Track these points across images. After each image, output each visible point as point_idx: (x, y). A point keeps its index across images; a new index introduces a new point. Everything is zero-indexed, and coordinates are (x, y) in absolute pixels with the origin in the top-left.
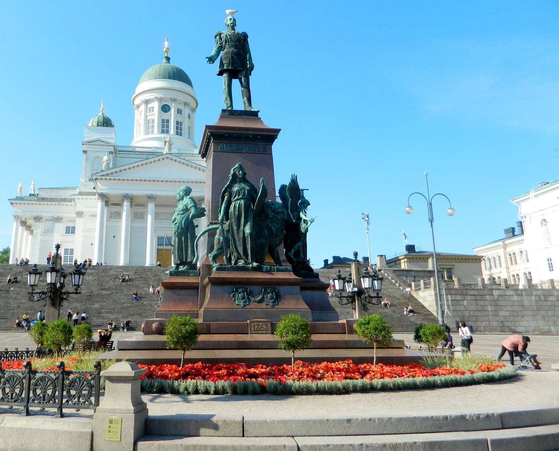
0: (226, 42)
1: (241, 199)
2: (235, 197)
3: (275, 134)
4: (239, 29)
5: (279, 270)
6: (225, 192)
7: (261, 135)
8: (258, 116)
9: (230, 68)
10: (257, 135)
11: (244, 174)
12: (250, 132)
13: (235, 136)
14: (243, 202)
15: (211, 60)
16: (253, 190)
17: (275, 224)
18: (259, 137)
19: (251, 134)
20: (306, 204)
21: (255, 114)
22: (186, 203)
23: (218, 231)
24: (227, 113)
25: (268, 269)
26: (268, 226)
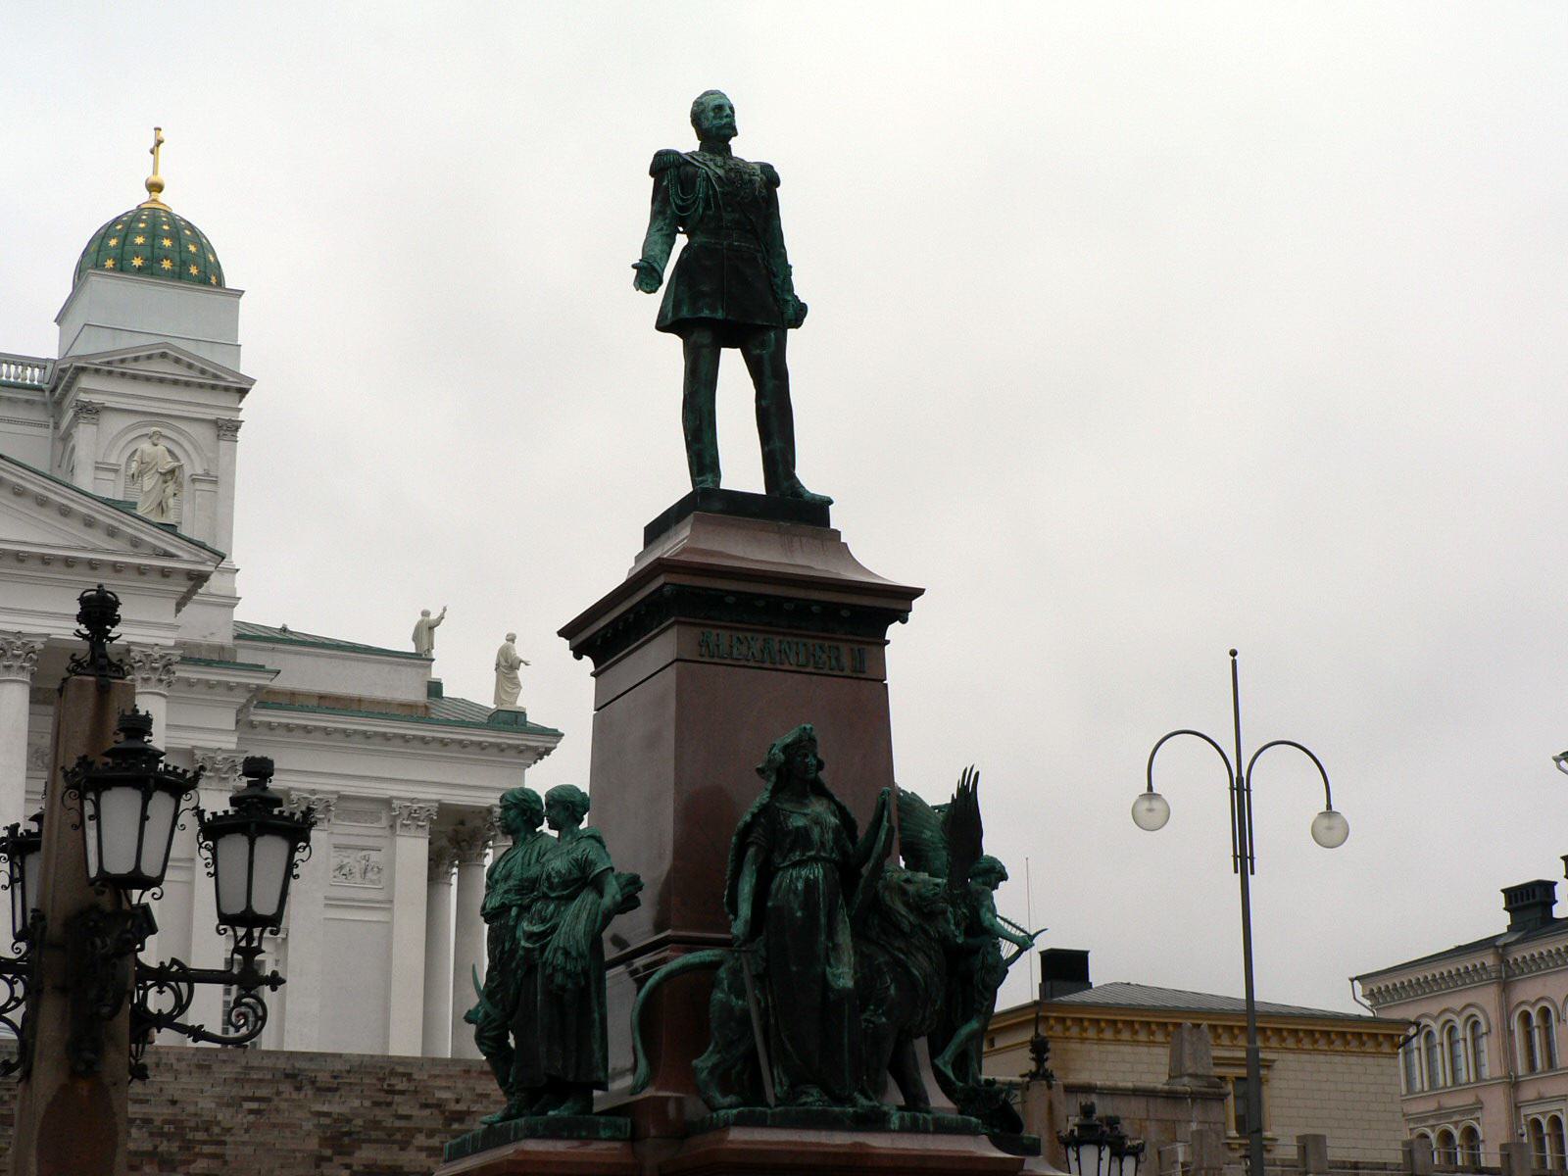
0: (707, 206)
1: (815, 859)
2: (792, 850)
3: (900, 606)
4: (743, 148)
5: (942, 1128)
6: (749, 828)
7: (852, 607)
8: (825, 520)
9: (720, 315)
11: (820, 765)
12: (816, 595)
14: (818, 872)
16: (847, 823)
17: (920, 956)
18: (845, 613)
19: (817, 602)
20: (996, 874)
21: (815, 512)
22: (578, 854)
23: (722, 973)
26: (898, 962)
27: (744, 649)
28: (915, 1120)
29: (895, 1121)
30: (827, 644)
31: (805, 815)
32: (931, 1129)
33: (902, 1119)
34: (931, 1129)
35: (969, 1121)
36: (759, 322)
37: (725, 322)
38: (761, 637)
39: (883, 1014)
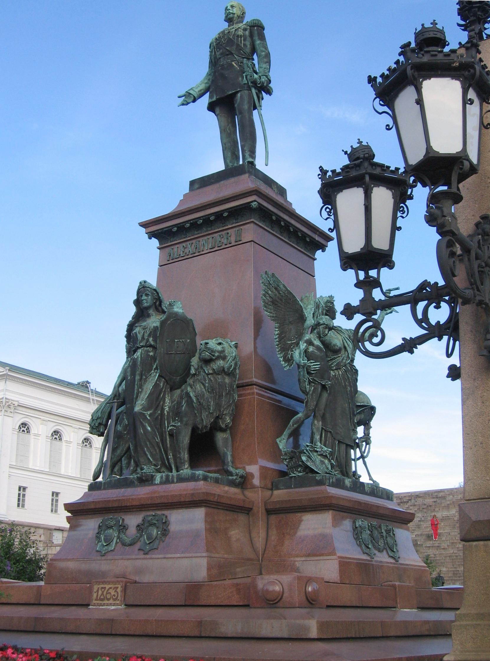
1: (138, 348)
5: (181, 480)
9: (214, 99)
10: (221, 213)
13: (188, 225)
15: (190, 98)
24: (196, 186)
25: (164, 477)
27: (187, 251)
28: (167, 476)
29: (158, 480)
30: (223, 233)
31: (140, 326)
32: (175, 480)
33: (162, 477)
34: (175, 480)
35: (195, 473)
36: (231, 93)
37: (218, 100)
38: (194, 241)
39: (179, 421)
